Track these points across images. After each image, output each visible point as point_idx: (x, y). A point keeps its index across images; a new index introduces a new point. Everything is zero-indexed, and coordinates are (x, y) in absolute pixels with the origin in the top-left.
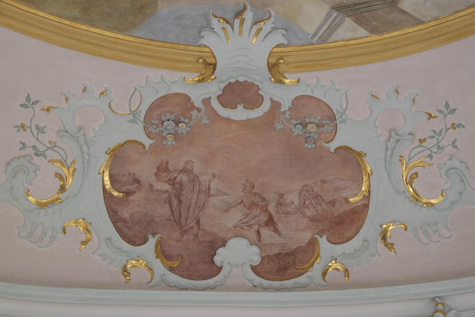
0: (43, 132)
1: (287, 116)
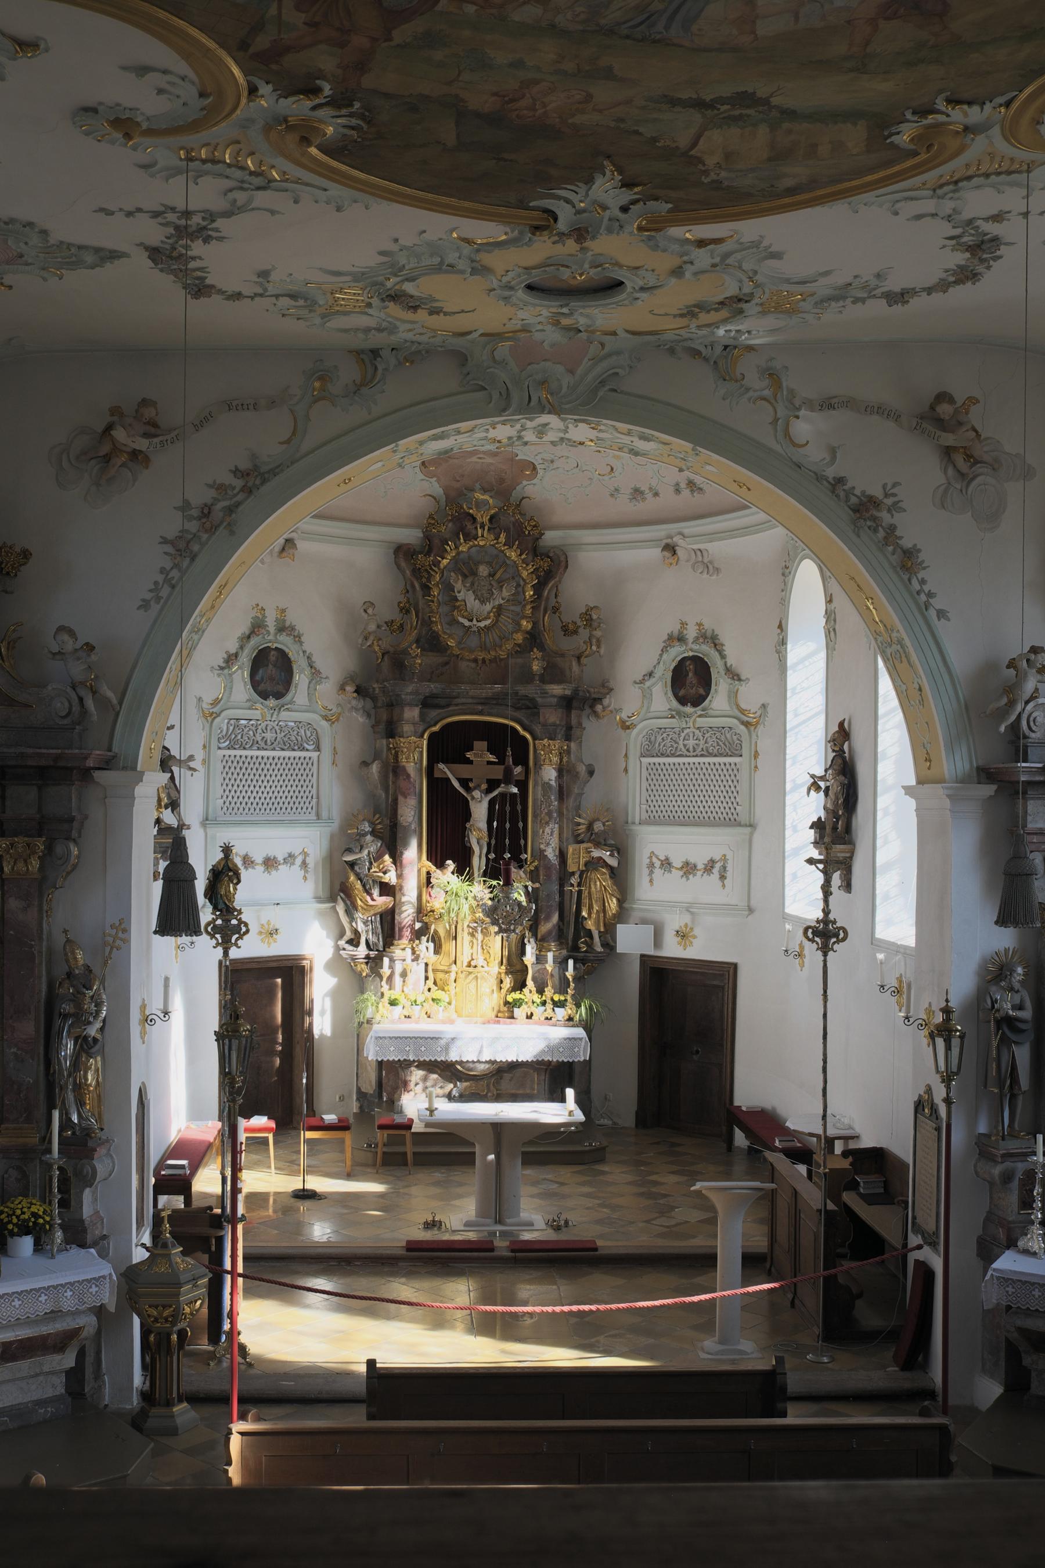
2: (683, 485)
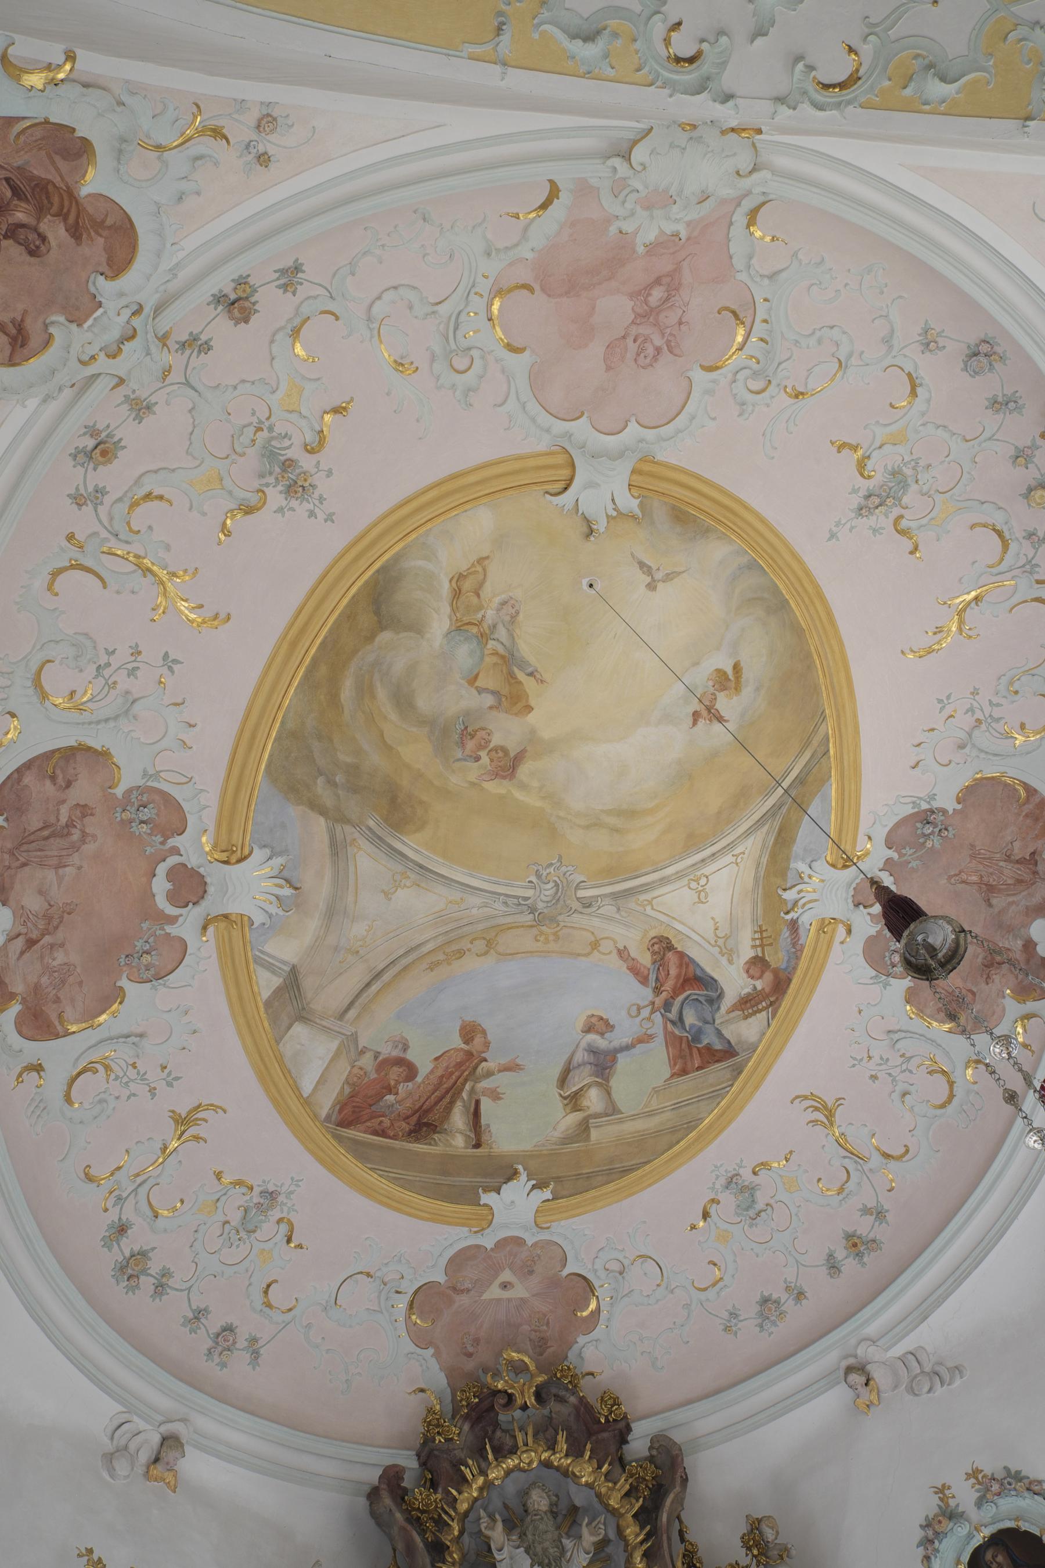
0: (129, 675)
1: (158, 932)
2: (840, 1254)
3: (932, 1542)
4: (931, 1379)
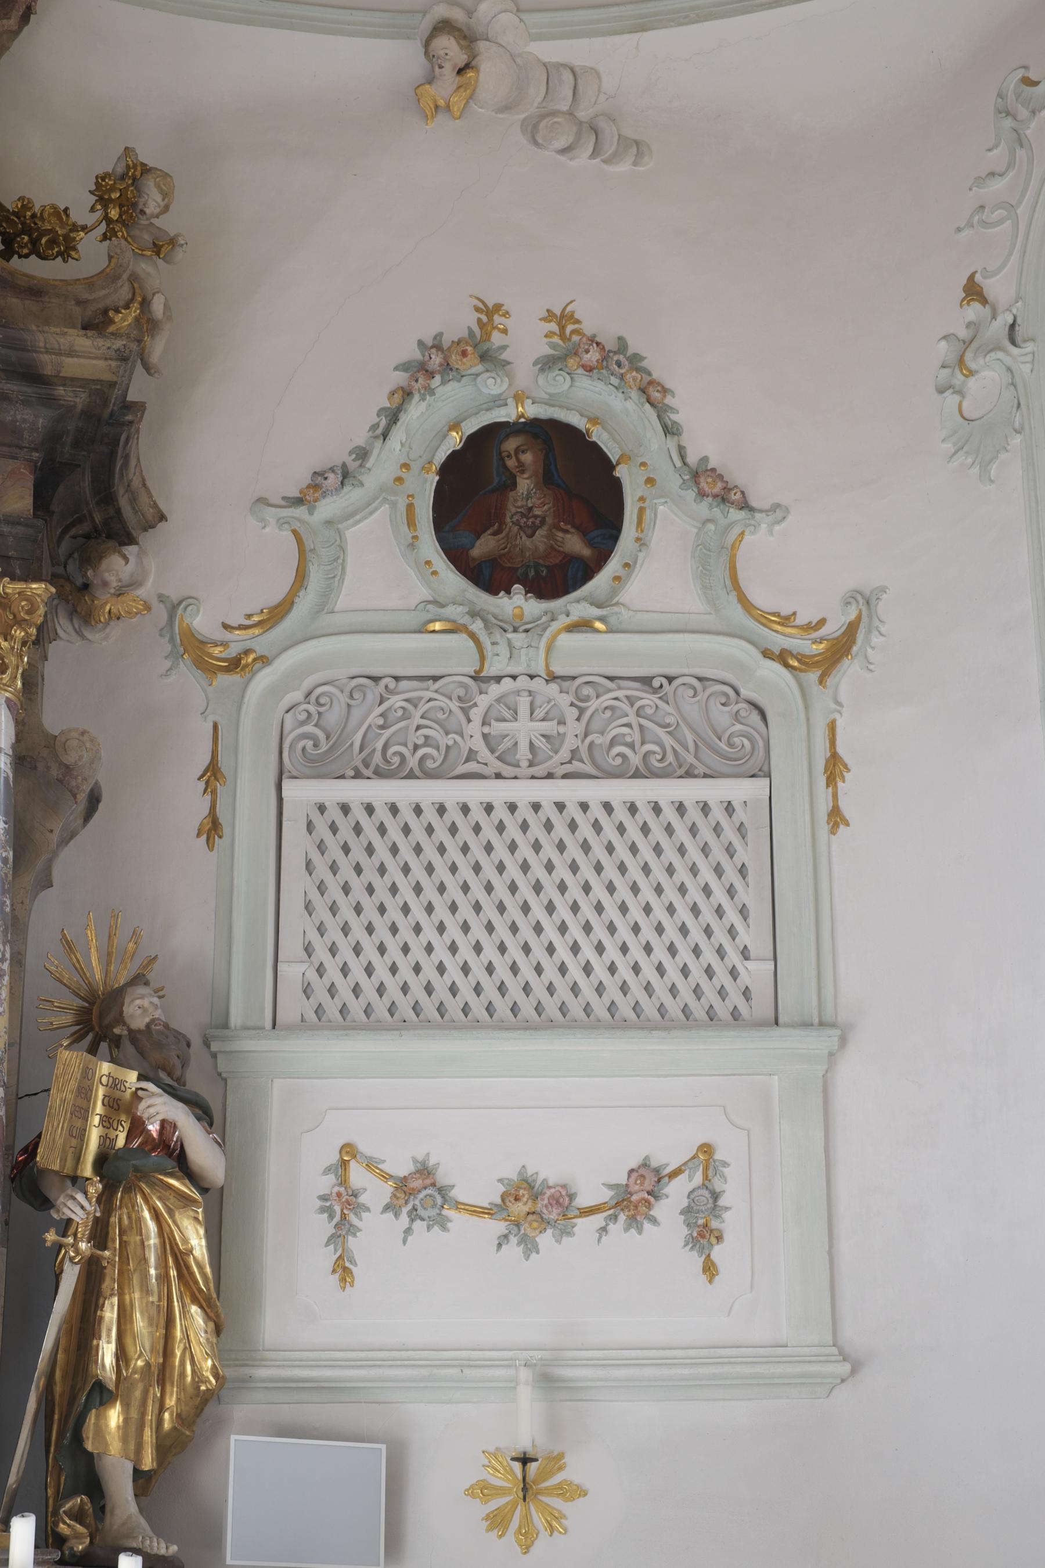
3: (431, 375)
4: (579, 135)
